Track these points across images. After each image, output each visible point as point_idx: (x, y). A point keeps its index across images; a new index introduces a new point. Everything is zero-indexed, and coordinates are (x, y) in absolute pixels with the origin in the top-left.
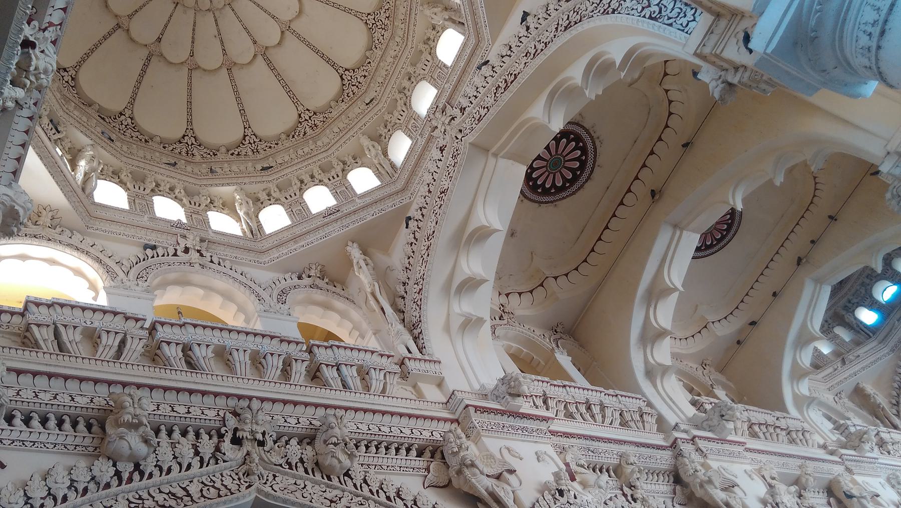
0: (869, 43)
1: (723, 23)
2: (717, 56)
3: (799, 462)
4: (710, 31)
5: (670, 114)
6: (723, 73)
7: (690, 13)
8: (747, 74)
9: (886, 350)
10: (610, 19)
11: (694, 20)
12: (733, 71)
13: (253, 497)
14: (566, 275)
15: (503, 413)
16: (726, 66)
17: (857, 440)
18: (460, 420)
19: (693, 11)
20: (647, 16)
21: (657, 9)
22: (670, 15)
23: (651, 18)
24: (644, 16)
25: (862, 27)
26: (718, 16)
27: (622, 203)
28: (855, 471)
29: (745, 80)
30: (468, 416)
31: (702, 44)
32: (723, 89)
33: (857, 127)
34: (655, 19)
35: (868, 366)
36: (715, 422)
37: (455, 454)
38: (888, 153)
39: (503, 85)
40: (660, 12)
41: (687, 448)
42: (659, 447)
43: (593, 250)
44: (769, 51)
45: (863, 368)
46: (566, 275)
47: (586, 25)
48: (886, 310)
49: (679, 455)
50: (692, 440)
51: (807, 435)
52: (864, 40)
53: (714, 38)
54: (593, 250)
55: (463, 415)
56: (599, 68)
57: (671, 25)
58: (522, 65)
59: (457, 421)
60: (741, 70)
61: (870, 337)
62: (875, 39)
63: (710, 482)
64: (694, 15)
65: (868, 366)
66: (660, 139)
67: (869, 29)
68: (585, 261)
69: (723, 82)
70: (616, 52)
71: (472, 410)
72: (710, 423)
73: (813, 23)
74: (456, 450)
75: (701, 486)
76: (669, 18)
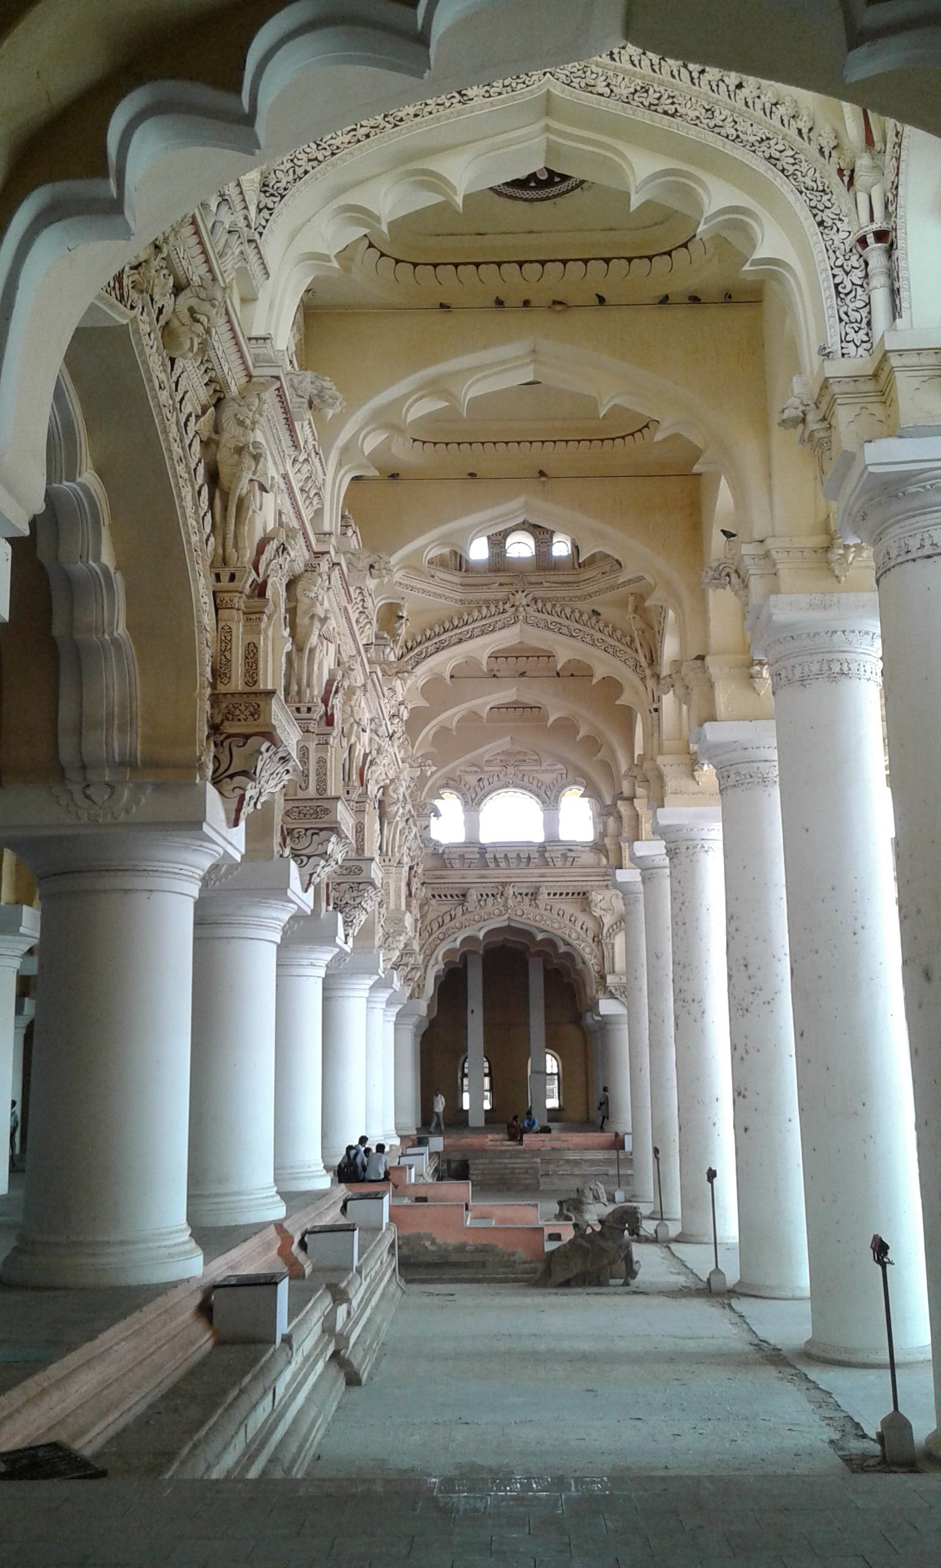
0: (914, 550)
1: (870, 386)
2: (833, 400)
3: (354, 653)
4: (855, 379)
5: (669, 253)
6: (813, 406)
7: (862, 336)
8: (822, 434)
9: (458, 596)
10: (809, 224)
11: (857, 347)
12: (821, 416)
13: (125, 322)
14: (382, 255)
15: (286, 411)
16: (823, 406)
17: (394, 671)
18: (254, 380)
19: (866, 338)
20: (837, 280)
21: (849, 287)
22: (850, 313)
23: (836, 286)
24: (834, 276)
25: (926, 535)
26: (875, 376)
27: (521, 264)
28: (368, 695)
29: (817, 435)
30: (265, 386)
31: (840, 379)
32: (798, 417)
33: (770, 492)
34: (838, 293)
35: (429, 593)
36: (360, 566)
37: (241, 423)
38: (762, 541)
39: (652, 97)
40: (847, 294)
41: (324, 566)
42: (309, 546)
43: (435, 266)
44: (871, 469)
45: (424, 591)
46: (382, 255)
47: (786, 188)
48: (499, 563)
49: (311, 568)
50: (334, 564)
51: (368, 626)
52: (914, 544)
53: (850, 387)
54: (435, 266)
55: (261, 380)
56: (737, 223)
57: (841, 320)
58: (693, 114)
59: (249, 376)
60: (825, 425)
61: (460, 570)
62: (920, 553)
63: (324, 620)
64: (863, 342)
65: (429, 593)
66: (629, 260)
67: (927, 542)
68: (415, 265)
69: (803, 412)
70: (771, 243)
71: (278, 385)
72: (354, 560)
73: (912, 489)
74: (248, 422)
75: (312, 617)
76: (846, 313)
